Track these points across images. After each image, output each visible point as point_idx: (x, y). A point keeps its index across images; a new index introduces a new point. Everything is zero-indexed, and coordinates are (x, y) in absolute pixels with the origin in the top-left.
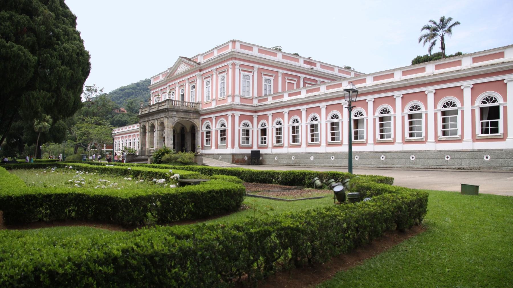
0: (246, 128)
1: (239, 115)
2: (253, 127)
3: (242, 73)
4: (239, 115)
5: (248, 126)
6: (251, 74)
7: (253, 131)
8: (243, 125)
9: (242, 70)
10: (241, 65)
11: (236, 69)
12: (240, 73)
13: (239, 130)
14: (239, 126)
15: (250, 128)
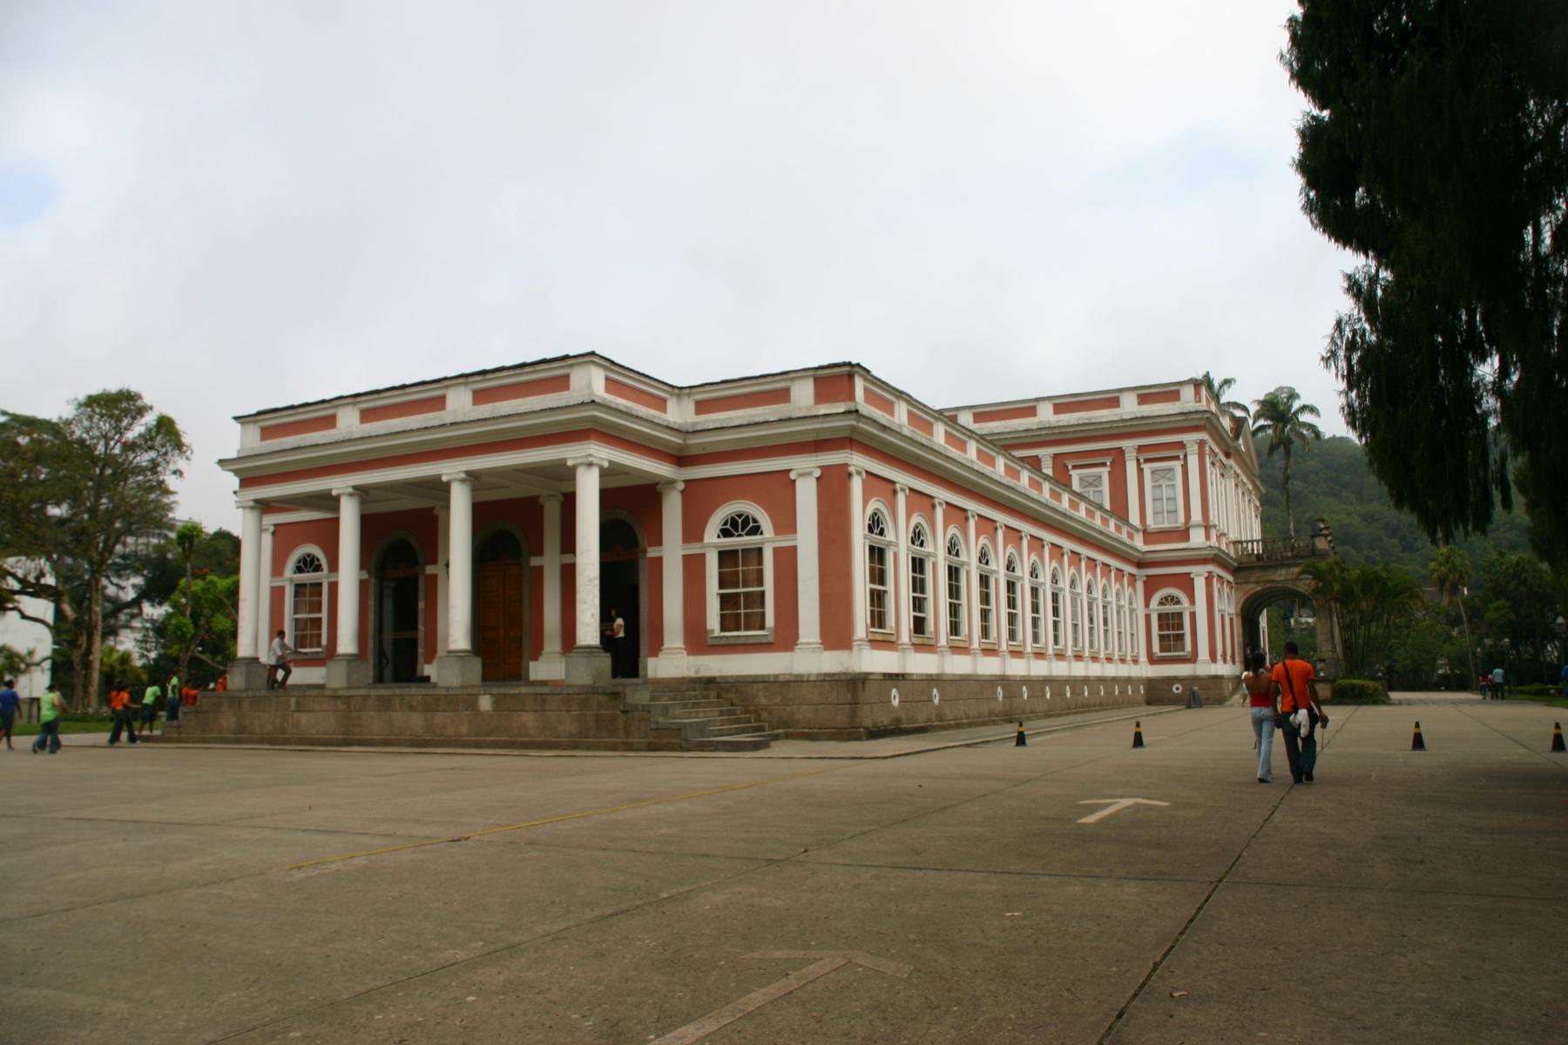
0: (1170, 608)
1: (1145, 578)
2: (1193, 602)
3: (1147, 468)
4: (1145, 578)
5: (1178, 602)
6: (1177, 465)
7: (1193, 616)
8: (1161, 603)
9: (1147, 461)
10: (1141, 449)
11: (1128, 463)
12: (1140, 471)
13: (1148, 617)
14: (1147, 604)
15: (1184, 609)
